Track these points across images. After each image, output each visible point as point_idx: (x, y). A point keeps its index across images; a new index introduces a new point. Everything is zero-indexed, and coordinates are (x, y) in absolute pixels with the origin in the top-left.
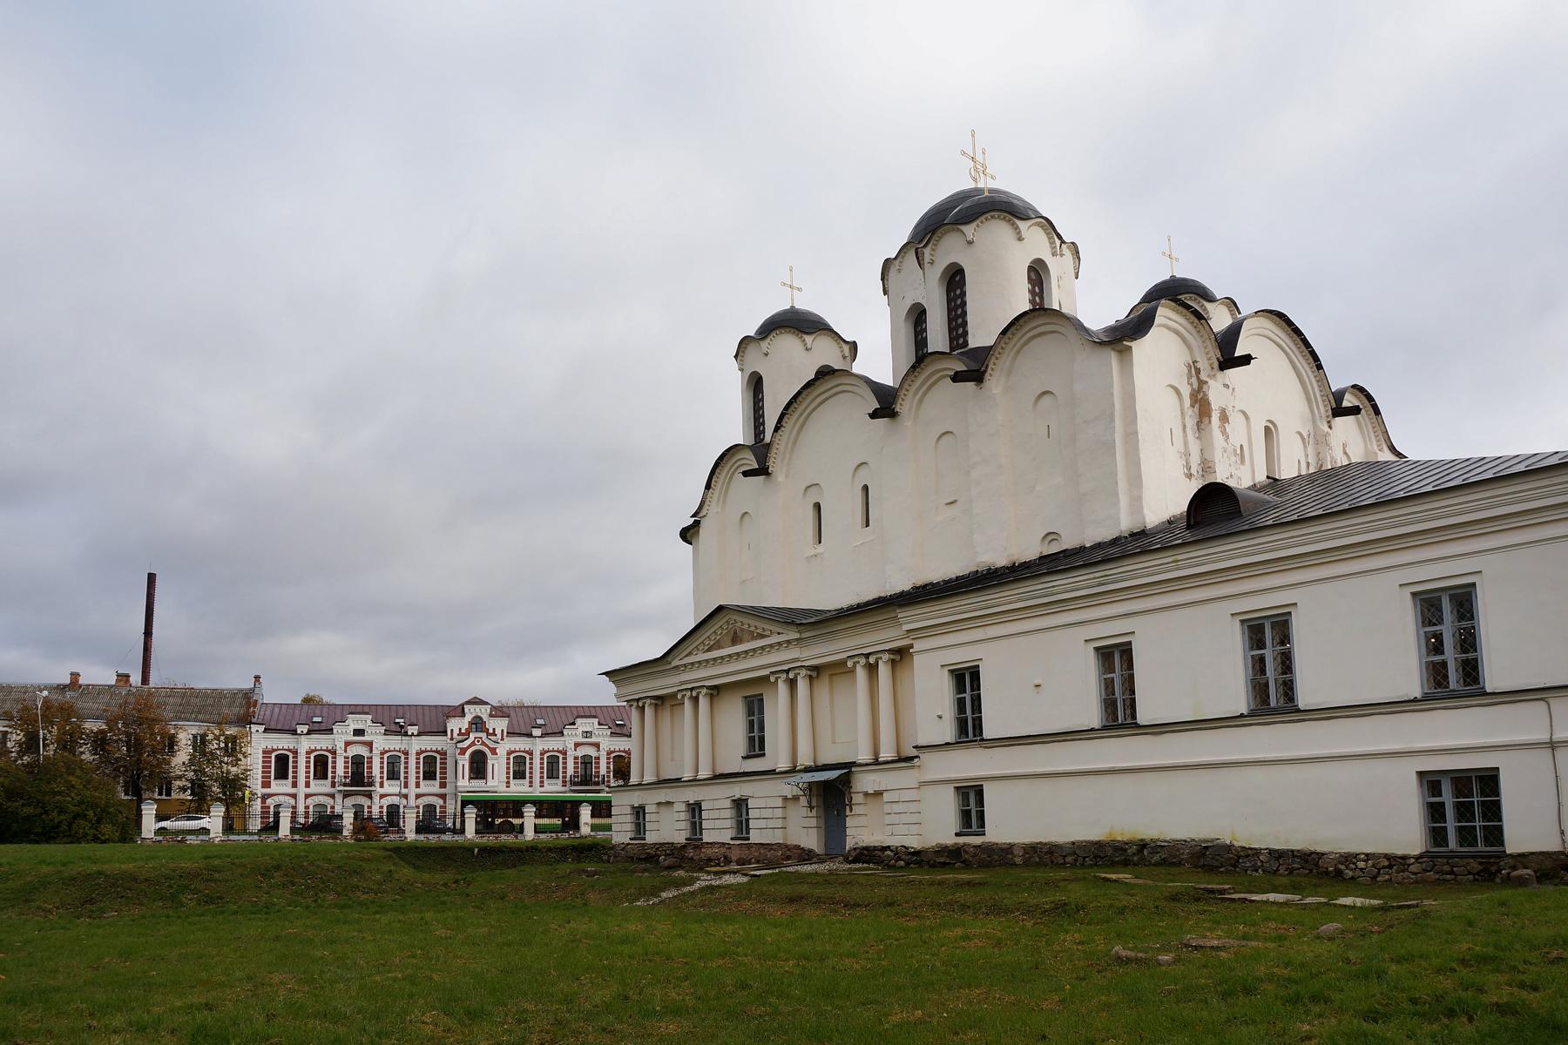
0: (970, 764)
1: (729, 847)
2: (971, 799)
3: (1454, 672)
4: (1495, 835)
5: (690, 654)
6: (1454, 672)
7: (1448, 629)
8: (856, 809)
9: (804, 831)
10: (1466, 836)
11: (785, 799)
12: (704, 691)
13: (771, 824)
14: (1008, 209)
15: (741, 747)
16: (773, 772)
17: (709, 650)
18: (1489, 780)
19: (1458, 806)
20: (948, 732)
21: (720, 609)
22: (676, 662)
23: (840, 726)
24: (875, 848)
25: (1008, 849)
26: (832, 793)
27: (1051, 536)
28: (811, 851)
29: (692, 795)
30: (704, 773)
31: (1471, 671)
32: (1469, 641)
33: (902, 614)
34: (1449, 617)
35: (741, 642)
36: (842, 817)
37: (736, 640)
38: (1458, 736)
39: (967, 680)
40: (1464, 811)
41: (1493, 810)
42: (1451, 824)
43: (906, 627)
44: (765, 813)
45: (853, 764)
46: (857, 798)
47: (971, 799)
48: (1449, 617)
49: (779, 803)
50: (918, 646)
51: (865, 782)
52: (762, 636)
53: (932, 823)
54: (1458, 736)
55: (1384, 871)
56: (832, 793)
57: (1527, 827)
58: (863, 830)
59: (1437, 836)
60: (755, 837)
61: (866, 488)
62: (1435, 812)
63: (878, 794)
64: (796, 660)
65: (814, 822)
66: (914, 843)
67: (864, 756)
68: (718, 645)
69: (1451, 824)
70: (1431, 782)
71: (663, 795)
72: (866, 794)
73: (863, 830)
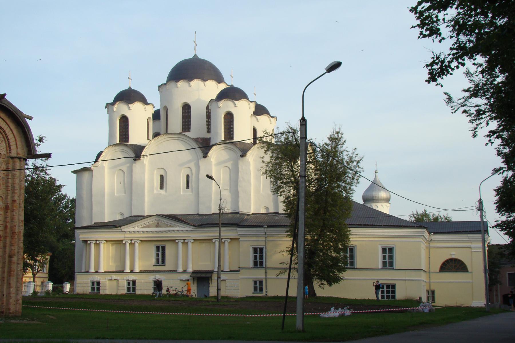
0: (259, 274)
4: (394, 297)
10: (388, 297)
12: (139, 242)
17: (142, 228)
18: (393, 286)
19: (387, 291)
20: (251, 265)
30: (137, 270)
31: (391, 264)
32: (391, 257)
33: (239, 230)
34: (388, 252)
35: (161, 227)
37: (157, 226)
38: (386, 277)
40: (388, 292)
41: (394, 292)
42: (385, 294)
43: (239, 233)
45: (212, 272)
48: (388, 252)
50: (241, 239)
52: (172, 227)
57: (400, 295)
64: (190, 237)
68: (148, 227)
69: (385, 294)
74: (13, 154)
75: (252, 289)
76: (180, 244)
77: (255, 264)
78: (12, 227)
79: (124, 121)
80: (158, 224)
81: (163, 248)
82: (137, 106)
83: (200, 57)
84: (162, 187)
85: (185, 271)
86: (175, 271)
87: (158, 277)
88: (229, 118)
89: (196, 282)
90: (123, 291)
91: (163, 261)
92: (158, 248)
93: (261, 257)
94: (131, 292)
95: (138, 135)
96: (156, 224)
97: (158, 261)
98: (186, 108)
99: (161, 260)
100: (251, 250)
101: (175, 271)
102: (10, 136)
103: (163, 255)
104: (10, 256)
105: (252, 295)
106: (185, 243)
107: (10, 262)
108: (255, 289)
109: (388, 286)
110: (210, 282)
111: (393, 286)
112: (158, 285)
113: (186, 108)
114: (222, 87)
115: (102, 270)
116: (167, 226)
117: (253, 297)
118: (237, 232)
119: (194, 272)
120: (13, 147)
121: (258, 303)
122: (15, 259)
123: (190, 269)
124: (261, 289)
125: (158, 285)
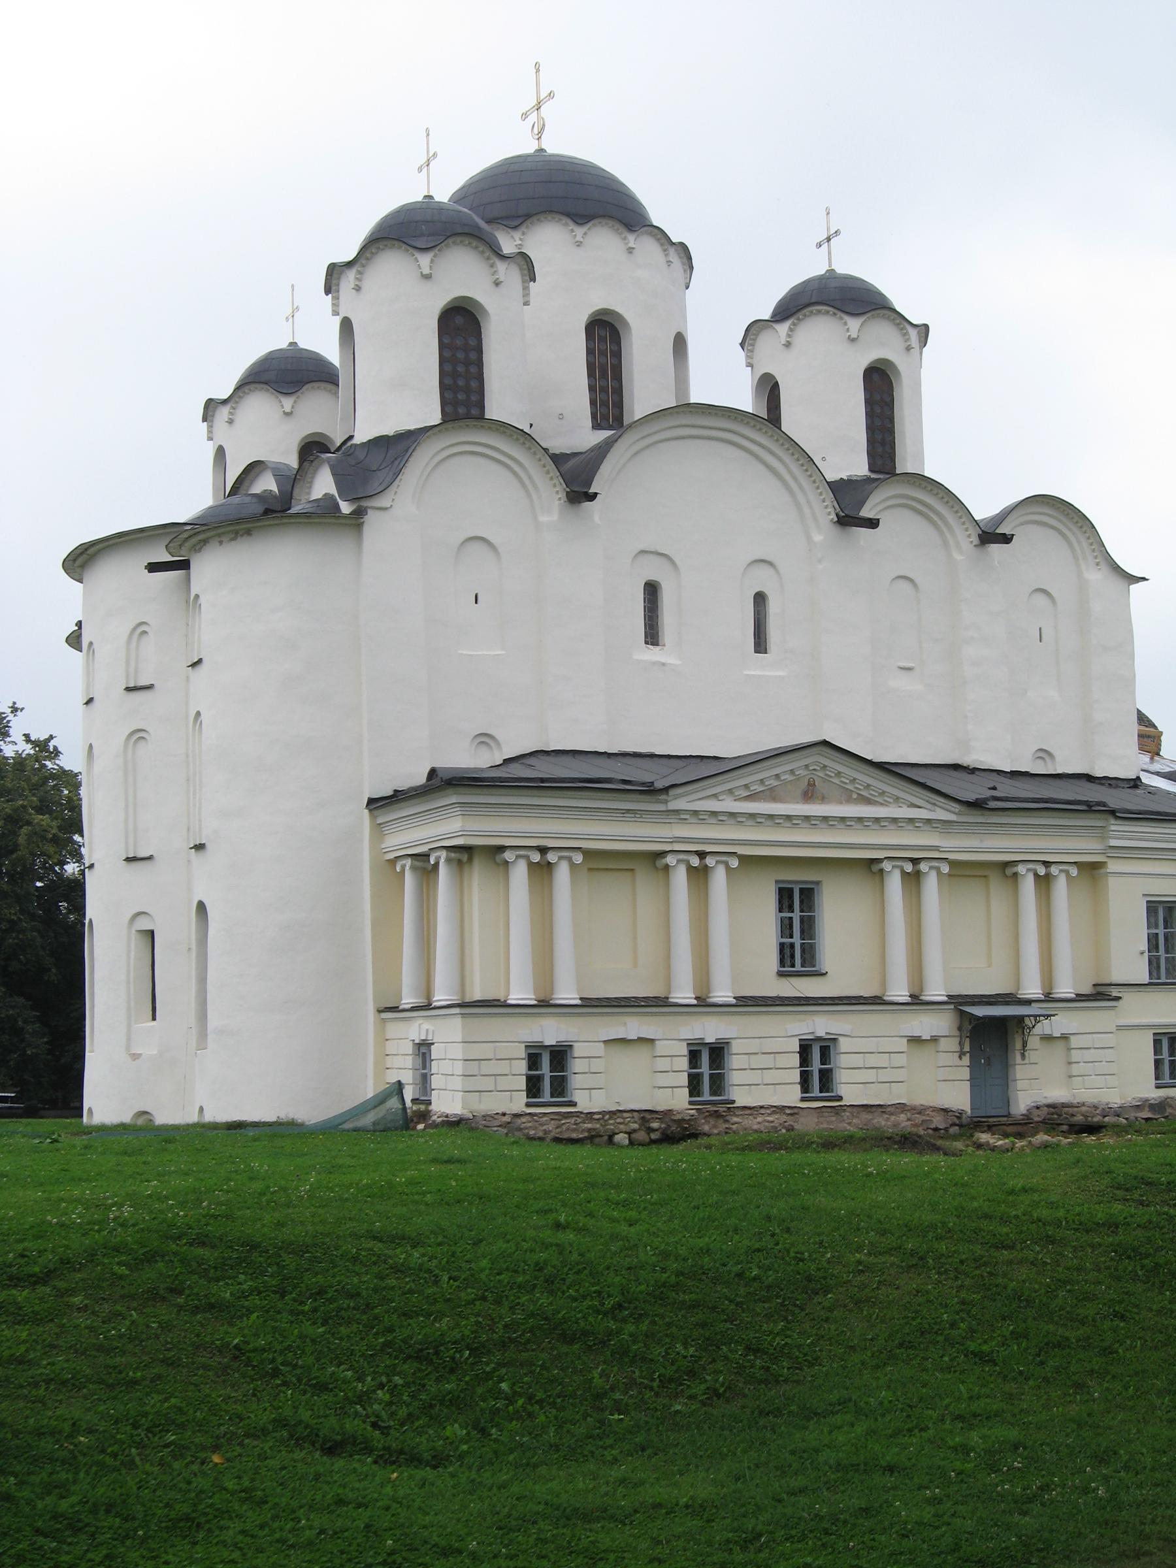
1: (794, 1111)
5: (715, 796)
8: (1031, 1056)
9: (945, 1085)
11: (915, 1040)
13: (884, 1076)
14: (582, 197)
17: (750, 798)
21: (825, 743)
22: (673, 805)
23: (965, 949)
24: (1064, 1105)
27: (1044, 754)
28: (961, 1113)
33: (1115, 826)
35: (823, 799)
36: (1006, 1067)
37: (809, 794)
44: (756, 1062)
46: (1033, 1042)
49: (903, 1045)
50: (1113, 866)
52: (868, 801)
56: (991, 1032)
58: (1037, 1084)
61: (760, 599)
63: (1065, 1037)
64: (936, 848)
65: (966, 1073)
67: (1032, 989)
68: (771, 795)
71: (633, 1026)
72: (1048, 1038)
73: (1037, 1084)
80: (811, 784)
81: (808, 895)
84: (652, 636)
85: (916, 1001)
86: (877, 1001)
87: (820, 1025)
89: (967, 1048)
92: (785, 896)
94: (707, 1096)
96: (804, 784)
97: (785, 954)
99: (798, 952)
101: (877, 1001)
103: (808, 927)
105: (1156, 1094)
110: (1018, 1045)
112: (817, 1061)
115: (567, 993)
116: (849, 797)
117: (1160, 1107)
118: (1104, 838)
123: (936, 991)
125: (817, 1061)
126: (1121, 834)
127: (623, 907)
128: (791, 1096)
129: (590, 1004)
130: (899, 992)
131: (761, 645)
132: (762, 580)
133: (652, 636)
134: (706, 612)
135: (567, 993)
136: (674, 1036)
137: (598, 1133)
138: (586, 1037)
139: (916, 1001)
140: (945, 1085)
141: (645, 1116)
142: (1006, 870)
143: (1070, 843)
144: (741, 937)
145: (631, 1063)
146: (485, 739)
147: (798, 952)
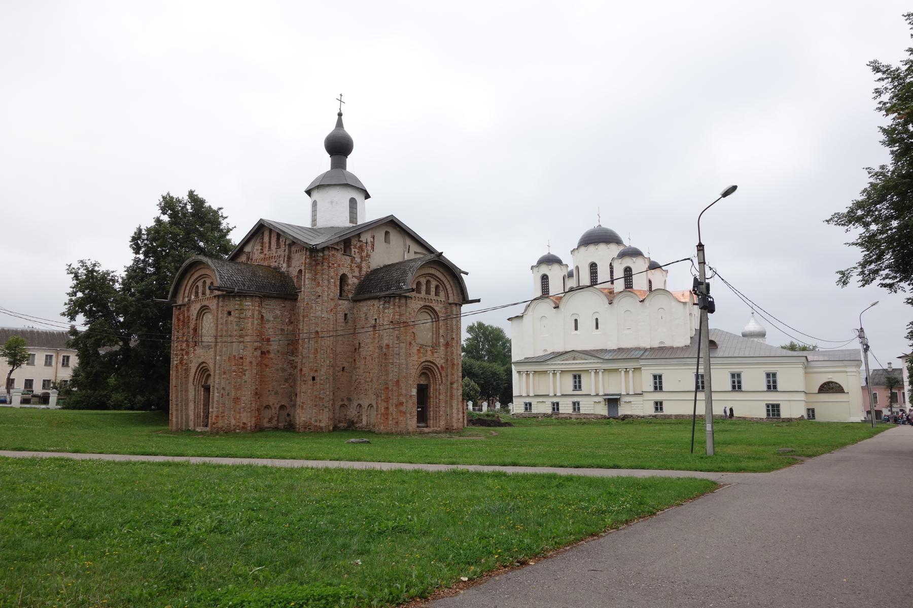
0: (658, 397)
2: (659, 405)
3: (772, 386)
4: (779, 415)
6: (772, 386)
7: (771, 379)
9: (603, 410)
10: (773, 415)
15: (572, 387)
16: (589, 395)
18: (778, 406)
20: (652, 389)
25: (669, 417)
26: (613, 402)
29: (555, 400)
37: (574, 359)
39: (658, 379)
40: (773, 411)
41: (779, 411)
45: (620, 395)
47: (659, 405)
51: (624, 399)
53: (648, 410)
54: (773, 398)
55: (759, 421)
56: (613, 402)
57: (785, 413)
58: (623, 410)
59: (768, 415)
60: (582, 411)
62: (768, 411)
66: (642, 414)
70: (768, 406)
71: (541, 399)
73: (623, 410)
74: (451, 301)
75: (654, 410)
76: (593, 373)
77: (656, 388)
78: (452, 360)
79: (545, 278)
81: (580, 377)
82: (556, 267)
83: (604, 226)
84: (576, 329)
87: (575, 399)
88: (628, 272)
90: (549, 411)
91: (580, 387)
92: (575, 377)
93: (661, 383)
95: (555, 287)
97: (575, 387)
98: (593, 267)
99: (578, 386)
100: (652, 378)
102: (448, 287)
103: (580, 382)
104: (452, 384)
106: (596, 372)
107: (452, 388)
108: (657, 409)
109: (773, 406)
111: (778, 406)
113: (593, 267)
114: (621, 248)
115: (531, 394)
117: (655, 416)
119: (606, 395)
120: (451, 295)
121: (659, 419)
122: (455, 386)
124: (661, 409)
126: (642, 362)
127: (542, 380)
128: (570, 411)
129: (563, 395)
130: (552, 394)
131: (597, 327)
132: (596, 316)
133: (576, 329)
134: (586, 323)
135: (531, 394)
136: (549, 402)
137: (536, 416)
138: (534, 401)
139: (597, 395)
140: (603, 410)
141: (544, 414)
142: (616, 370)
143: (631, 365)
144: (568, 383)
145: (540, 405)
146: (545, 350)
147: (578, 386)
